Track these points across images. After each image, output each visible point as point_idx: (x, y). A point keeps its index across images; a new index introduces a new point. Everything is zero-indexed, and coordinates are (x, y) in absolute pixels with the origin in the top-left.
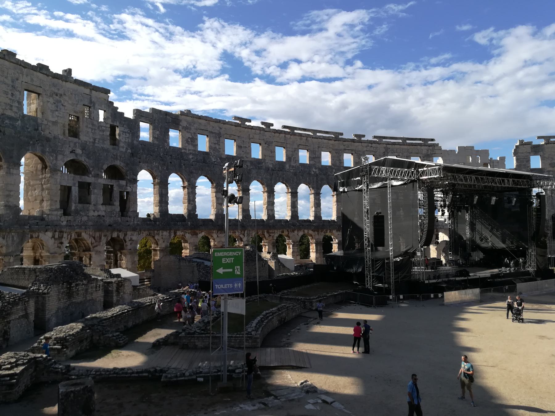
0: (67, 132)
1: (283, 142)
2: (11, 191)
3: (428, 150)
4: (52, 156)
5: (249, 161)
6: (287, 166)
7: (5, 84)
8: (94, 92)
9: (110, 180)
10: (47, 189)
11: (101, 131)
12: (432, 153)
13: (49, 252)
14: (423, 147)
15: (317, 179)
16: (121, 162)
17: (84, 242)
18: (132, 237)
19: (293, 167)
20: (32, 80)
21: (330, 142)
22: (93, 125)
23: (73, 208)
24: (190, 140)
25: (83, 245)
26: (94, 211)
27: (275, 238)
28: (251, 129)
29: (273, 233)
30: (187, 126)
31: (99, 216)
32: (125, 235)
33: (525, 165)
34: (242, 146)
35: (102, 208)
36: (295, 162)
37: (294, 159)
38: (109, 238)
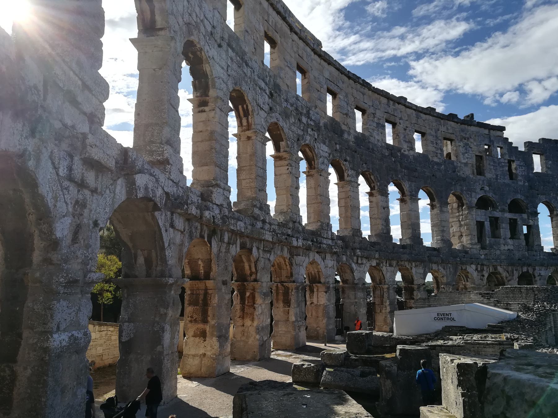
0: (475, 171)
2: (444, 227)
4: (468, 194)
7: (431, 135)
8: (492, 131)
9: (514, 214)
10: (466, 225)
11: (501, 167)
13: (474, 284)
16: (522, 196)
17: (499, 276)
18: (540, 272)
20: (447, 129)
22: (494, 162)
23: (488, 242)
25: (496, 280)
26: (504, 245)
31: (509, 250)
32: (534, 270)
35: (510, 242)
38: (521, 273)
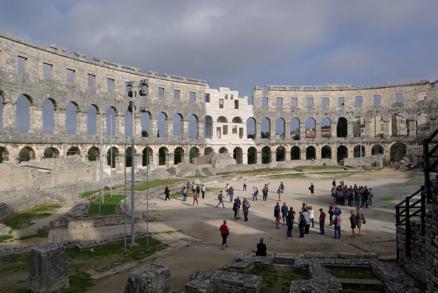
1: (94, 71)
3: (200, 88)
5: (64, 84)
6: (97, 91)
14: (197, 86)
15: (121, 104)
19: (102, 92)
21: (131, 75)
24: (9, 61)
27: (88, 151)
28: (67, 57)
29: (86, 146)
30: (7, 48)
33: (259, 103)
34: (59, 71)
36: (104, 89)
37: (103, 86)
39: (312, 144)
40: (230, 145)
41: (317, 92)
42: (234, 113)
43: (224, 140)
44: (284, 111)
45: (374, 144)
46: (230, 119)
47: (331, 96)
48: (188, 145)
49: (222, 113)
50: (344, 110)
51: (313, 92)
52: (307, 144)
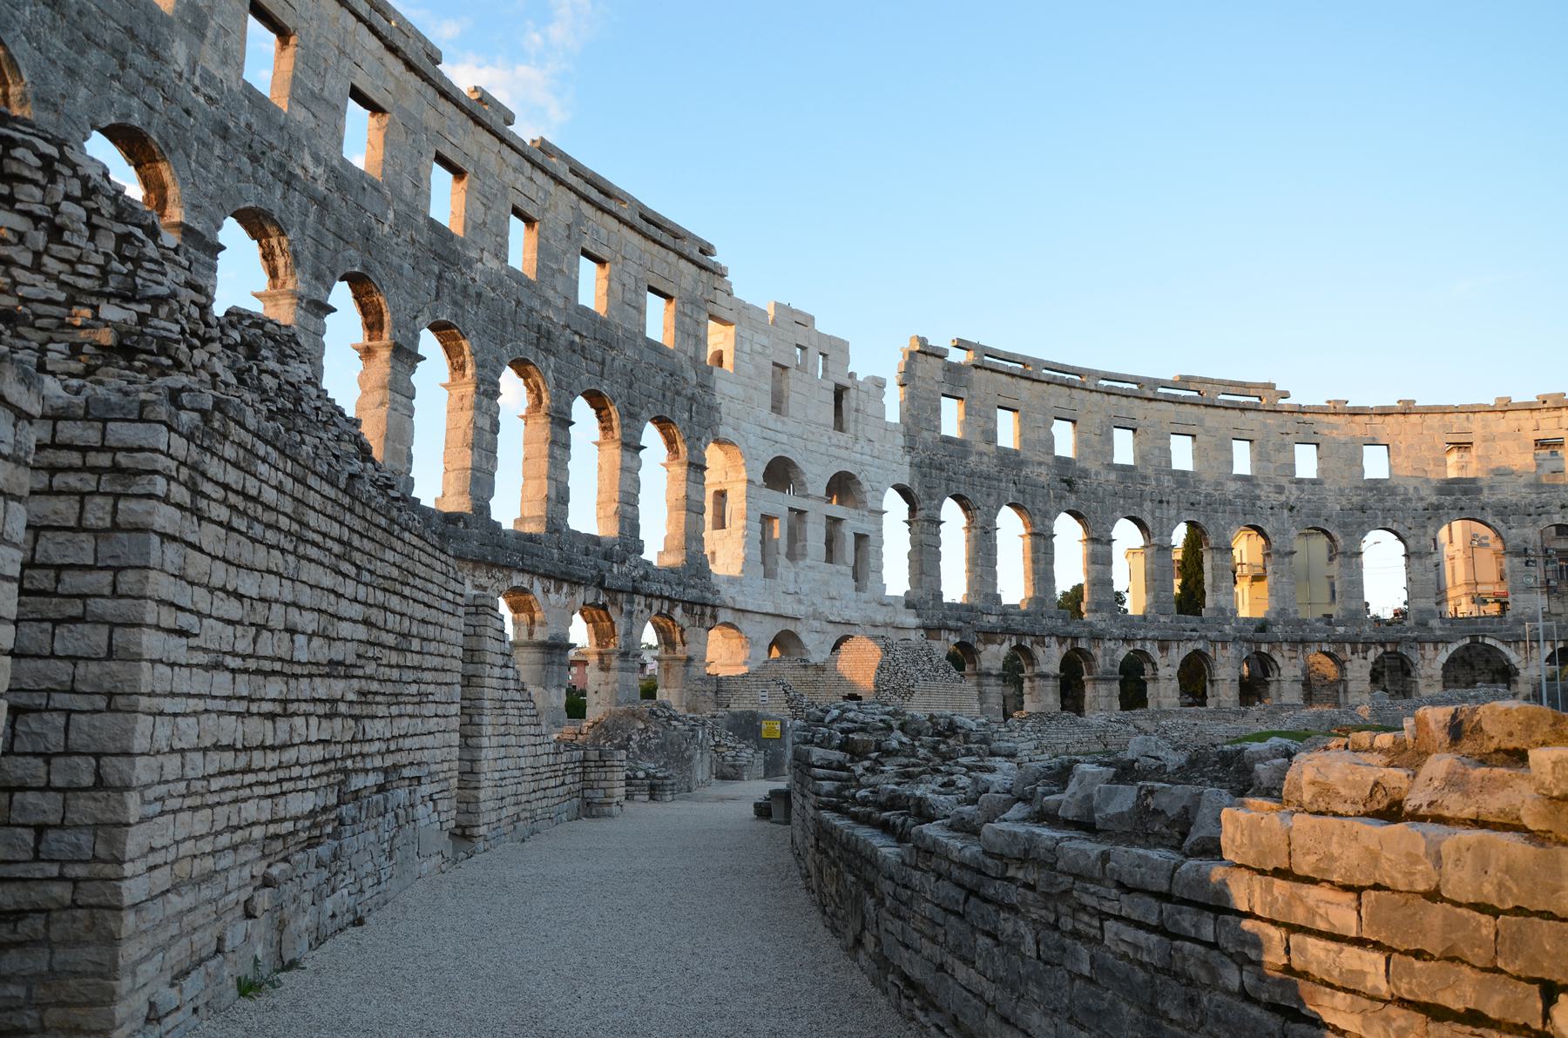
12: (706, 296)
14: (683, 263)
15: (320, 220)
39: (1144, 639)
40: (816, 624)
41: (1154, 404)
42: (833, 450)
43: (792, 591)
44: (1026, 477)
45: (1381, 650)
46: (816, 476)
47: (1207, 432)
48: (637, 598)
49: (784, 438)
50: (1258, 498)
51: (1137, 402)
52: (1127, 640)
